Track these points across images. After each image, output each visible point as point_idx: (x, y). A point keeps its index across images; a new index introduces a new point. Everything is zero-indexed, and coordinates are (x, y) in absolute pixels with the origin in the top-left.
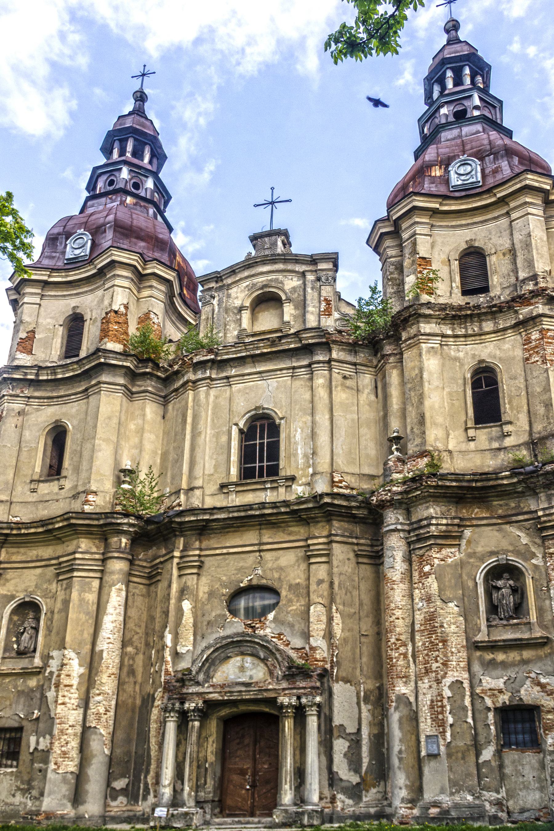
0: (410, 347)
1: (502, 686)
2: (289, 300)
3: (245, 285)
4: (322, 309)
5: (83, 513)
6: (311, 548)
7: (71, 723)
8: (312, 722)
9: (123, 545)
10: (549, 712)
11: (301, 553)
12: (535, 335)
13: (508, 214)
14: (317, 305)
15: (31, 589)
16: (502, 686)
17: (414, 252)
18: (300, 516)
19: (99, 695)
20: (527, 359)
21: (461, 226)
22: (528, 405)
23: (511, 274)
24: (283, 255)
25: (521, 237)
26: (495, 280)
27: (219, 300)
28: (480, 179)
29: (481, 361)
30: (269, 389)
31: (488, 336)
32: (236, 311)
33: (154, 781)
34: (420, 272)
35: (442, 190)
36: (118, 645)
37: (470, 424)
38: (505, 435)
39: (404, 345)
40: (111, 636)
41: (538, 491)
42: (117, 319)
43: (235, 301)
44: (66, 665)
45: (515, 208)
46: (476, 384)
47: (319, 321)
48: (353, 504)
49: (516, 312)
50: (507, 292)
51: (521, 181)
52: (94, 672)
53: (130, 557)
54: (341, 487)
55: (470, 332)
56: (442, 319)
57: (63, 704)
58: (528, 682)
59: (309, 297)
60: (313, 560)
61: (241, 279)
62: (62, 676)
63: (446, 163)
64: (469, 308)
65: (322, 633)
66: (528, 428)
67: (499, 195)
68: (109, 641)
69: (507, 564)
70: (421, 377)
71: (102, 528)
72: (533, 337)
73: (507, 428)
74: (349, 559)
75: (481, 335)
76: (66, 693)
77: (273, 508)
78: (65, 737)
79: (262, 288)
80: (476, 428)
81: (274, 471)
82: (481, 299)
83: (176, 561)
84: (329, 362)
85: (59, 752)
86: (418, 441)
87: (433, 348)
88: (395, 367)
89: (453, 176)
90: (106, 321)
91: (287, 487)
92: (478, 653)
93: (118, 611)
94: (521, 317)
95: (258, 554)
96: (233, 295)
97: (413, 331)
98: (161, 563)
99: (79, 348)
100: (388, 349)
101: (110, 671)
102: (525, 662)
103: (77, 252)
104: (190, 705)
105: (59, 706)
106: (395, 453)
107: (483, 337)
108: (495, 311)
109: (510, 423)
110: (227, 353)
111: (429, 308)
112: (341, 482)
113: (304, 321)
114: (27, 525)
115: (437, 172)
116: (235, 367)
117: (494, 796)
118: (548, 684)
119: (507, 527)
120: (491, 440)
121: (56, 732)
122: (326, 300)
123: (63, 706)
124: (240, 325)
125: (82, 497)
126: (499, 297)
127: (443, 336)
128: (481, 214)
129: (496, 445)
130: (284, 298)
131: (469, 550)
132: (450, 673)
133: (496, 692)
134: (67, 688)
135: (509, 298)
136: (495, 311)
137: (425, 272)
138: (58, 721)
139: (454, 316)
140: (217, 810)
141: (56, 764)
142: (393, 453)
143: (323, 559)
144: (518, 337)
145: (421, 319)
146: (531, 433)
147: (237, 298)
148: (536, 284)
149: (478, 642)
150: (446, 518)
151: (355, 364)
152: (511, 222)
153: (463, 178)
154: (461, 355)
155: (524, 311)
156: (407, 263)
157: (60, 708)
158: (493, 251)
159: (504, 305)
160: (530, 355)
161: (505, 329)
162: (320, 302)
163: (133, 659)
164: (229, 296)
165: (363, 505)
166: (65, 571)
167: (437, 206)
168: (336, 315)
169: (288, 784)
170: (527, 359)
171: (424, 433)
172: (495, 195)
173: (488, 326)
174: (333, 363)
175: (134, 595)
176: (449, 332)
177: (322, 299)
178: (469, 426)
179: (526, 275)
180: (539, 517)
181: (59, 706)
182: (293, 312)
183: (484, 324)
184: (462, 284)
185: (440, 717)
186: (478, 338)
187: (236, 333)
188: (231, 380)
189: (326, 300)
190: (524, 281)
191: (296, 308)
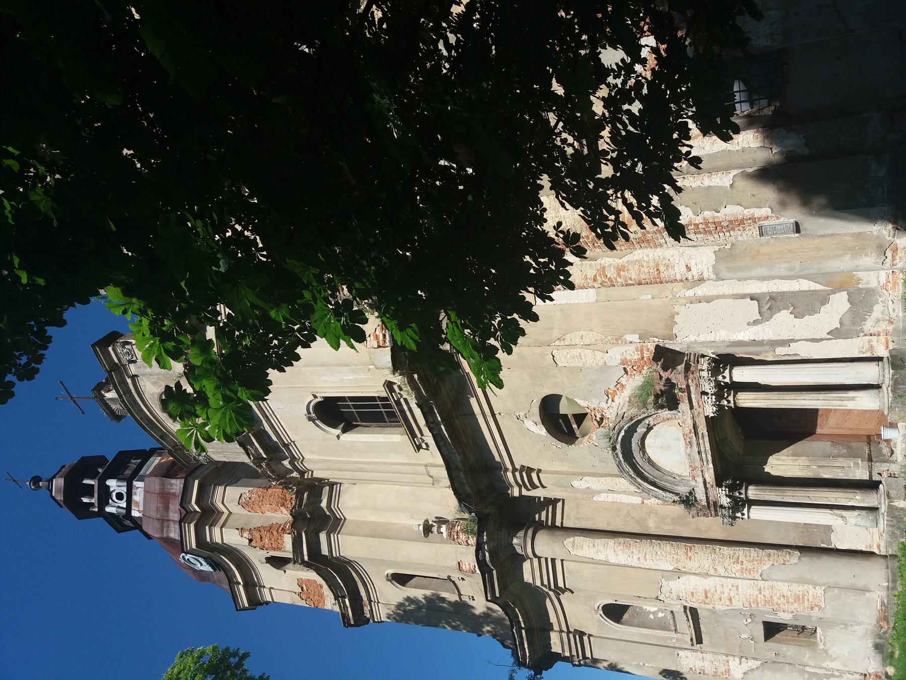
57: (730, 600)
68: (642, 559)
76: (716, 597)
78: (775, 598)
83: (525, 492)
85: (796, 605)
93: (601, 548)
101: (683, 558)
141: (812, 609)
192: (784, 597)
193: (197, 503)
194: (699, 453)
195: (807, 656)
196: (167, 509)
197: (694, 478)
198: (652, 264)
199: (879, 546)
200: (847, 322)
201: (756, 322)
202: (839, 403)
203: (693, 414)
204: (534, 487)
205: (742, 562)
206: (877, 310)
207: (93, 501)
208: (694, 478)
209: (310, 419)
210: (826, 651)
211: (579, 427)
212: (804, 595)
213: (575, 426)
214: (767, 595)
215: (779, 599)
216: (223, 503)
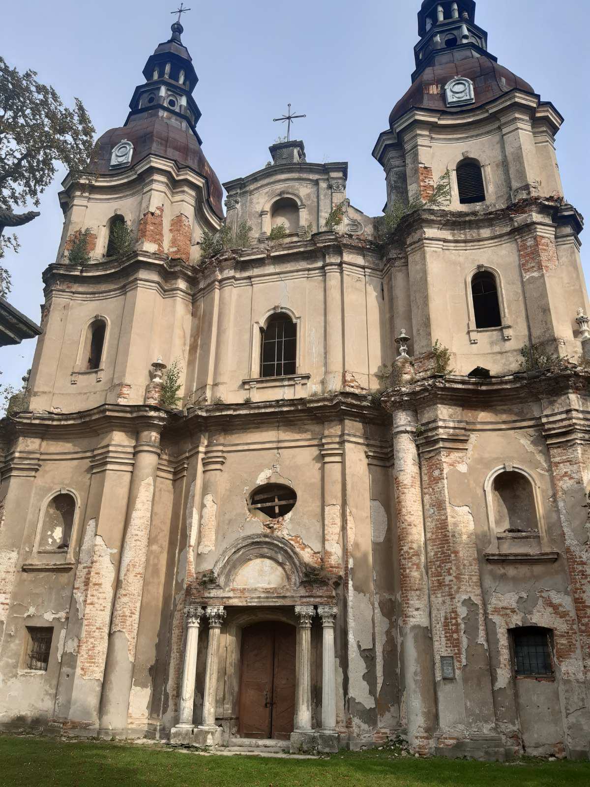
0: (414, 251)
1: (514, 605)
3: (265, 191)
5: (118, 405)
6: (326, 447)
7: (98, 625)
8: (329, 636)
9: (153, 438)
10: (562, 636)
11: (315, 451)
12: (530, 242)
13: (499, 128)
15: (67, 482)
16: (514, 605)
18: (315, 415)
19: (125, 595)
20: (524, 265)
22: (526, 310)
24: (299, 164)
25: (512, 150)
27: (242, 205)
28: (473, 96)
30: (288, 290)
31: (486, 242)
33: (175, 693)
34: (423, 181)
35: (439, 105)
36: (145, 542)
37: (473, 326)
38: (506, 339)
39: (409, 249)
41: (540, 396)
43: (257, 206)
44: (96, 562)
49: (511, 219)
53: (159, 451)
54: (352, 387)
55: (469, 238)
56: (444, 225)
57: (92, 604)
58: (540, 602)
59: (321, 203)
60: (327, 459)
62: (92, 574)
63: (442, 82)
65: (336, 537)
66: (526, 333)
67: (491, 111)
68: (137, 538)
69: (514, 472)
70: (426, 280)
71: (135, 422)
72: (528, 244)
73: (507, 332)
74: (360, 460)
75: (479, 241)
76: (95, 593)
77: (290, 405)
78: (92, 640)
79: (280, 195)
80: (478, 332)
81: (291, 368)
82: (478, 206)
84: (340, 265)
86: (424, 343)
87: (436, 252)
88: (400, 271)
89: (449, 94)
91: (303, 385)
92: (490, 567)
93: (146, 507)
94: (516, 224)
95: (276, 451)
96: (255, 201)
97: (416, 236)
98: (187, 458)
100: (393, 254)
102: (537, 578)
103: (120, 159)
104: (211, 611)
105: (87, 606)
106: (403, 354)
107: (481, 243)
108: (490, 219)
109: (509, 327)
110: (249, 255)
111: (432, 214)
112: (352, 381)
114: (67, 417)
115: (434, 90)
116: (257, 267)
117: (511, 728)
118: (560, 605)
119: (512, 432)
120: (492, 343)
121: (83, 634)
123: (91, 606)
125: (117, 390)
126: (495, 206)
127: (445, 241)
129: (497, 349)
130: (299, 203)
131: (476, 456)
132: (464, 588)
133: (508, 611)
134: (97, 587)
136: (490, 219)
137: (427, 180)
138: (85, 622)
139: (454, 222)
140: (234, 730)
141: (82, 669)
142: (401, 354)
143: (338, 459)
144: (514, 245)
145: (423, 225)
147: (258, 203)
148: (529, 193)
149: (489, 555)
150: (454, 421)
153: (457, 95)
154: (461, 259)
155: (520, 219)
157: (89, 609)
160: (527, 261)
161: (501, 236)
163: (158, 559)
166: (98, 464)
167: (435, 120)
169: (306, 704)
171: (429, 334)
173: (485, 232)
174: (344, 265)
175: (160, 490)
176: (450, 238)
178: (471, 329)
179: (519, 185)
180: (543, 424)
181: (87, 606)
182: (308, 217)
183: (482, 231)
185: (455, 636)
186: (476, 243)
188: (252, 280)
190: (517, 190)
191: (310, 213)
192: (93, 647)
194: (259, 597)
195: (10, 661)
196: (176, 148)
197: (233, 590)
198: (421, 586)
199: (132, 723)
200: (359, 707)
201: (359, 646)
202: (305, 700)
203: (297, 597)
204: (204, 465)
205: (130, 617)
206: (365, 726)
207: (166, 76)
208: (233, 590)
209: (274, 309)
210: (15, 676)
211: (258, 509)
212: (94, 663)
213: (259, 505)
214: (97, 634)
215: (92, 643)
216: (183, 201)
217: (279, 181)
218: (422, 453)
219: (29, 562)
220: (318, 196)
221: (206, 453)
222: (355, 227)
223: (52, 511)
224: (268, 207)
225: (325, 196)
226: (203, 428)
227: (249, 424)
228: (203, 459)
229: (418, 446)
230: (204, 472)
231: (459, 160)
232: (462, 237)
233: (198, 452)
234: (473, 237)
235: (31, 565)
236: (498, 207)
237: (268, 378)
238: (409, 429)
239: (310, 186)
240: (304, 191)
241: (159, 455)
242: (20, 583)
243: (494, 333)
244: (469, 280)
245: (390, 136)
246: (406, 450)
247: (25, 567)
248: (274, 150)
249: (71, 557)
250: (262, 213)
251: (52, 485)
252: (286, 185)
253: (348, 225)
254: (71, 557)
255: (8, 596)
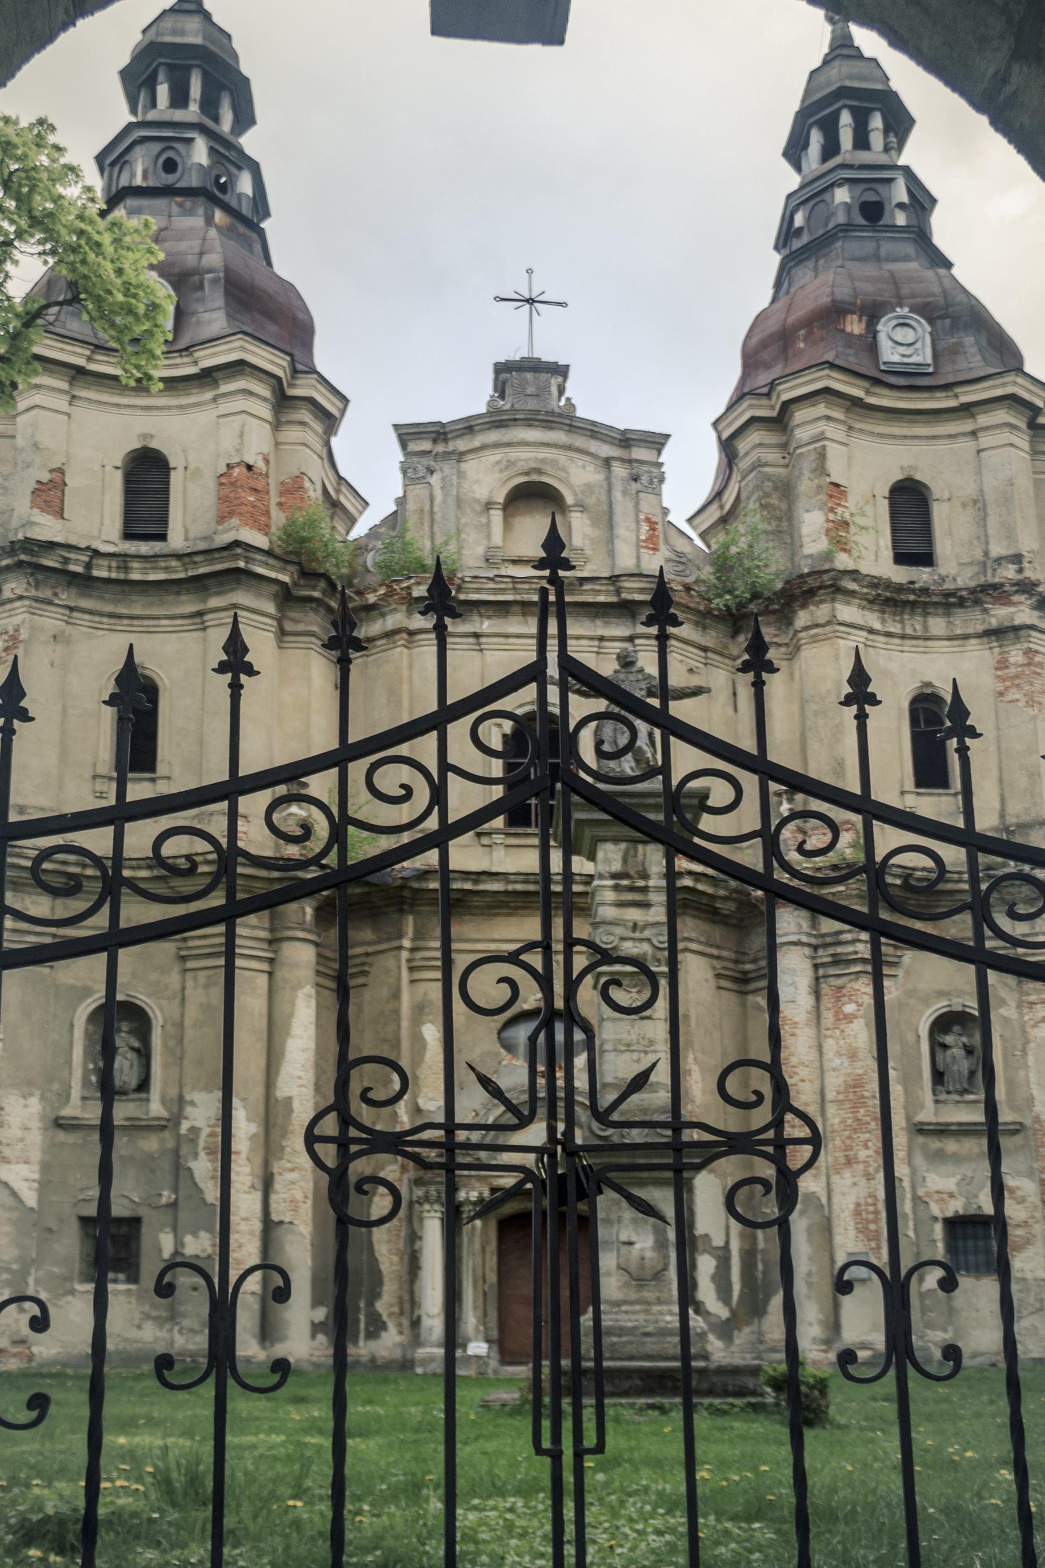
2: (582, 507)
4: (643, 537)
14: (633, 526)
17: (821, 468)
20: (1001, 694)
21: (894, 437)
23: (975, 542)
26: (944, 546)
29: (929, 684)
32: (478, 508)
40: (301, 1074)
42: (253, 483)
45: (987, 428)
46: (914, 721)
47: (638, 557)
48: (722, 892)
49: (986, 611)
50: (969, 572)
51: (1004, 385)
52: (275, 1134)
59: (618, 509)
61: (484, 447)
64: (913, 591)
68: (300, 1082)
75: (927, 639)
80: (918, 794)
82: (923, 576)
90: (225, 479)
99: (164, 520)
107: (930, 643)
113: (612, 554)
122: (648, 520)
124: (489, 537)
126: (955, 580)
128: (927, 423)
130: (569, 500)
135: (972, 584)
144: (987, 653)
146: (1002, 816)
151: (705, 649)
152: (979, 452)
156: (805, 485)
158: (946, 496)
159: (964, 593)
160: (1006, 688)
161: (966, 637)
162: (638, 522)
164: (461, 475)
165: (734, 895)
168: (664, 552)
170: (1001, 694)
172: (956, 396)
173: (937, 625)
177: (642, 517)
178: (907, 788)
182: (589, 530)
184: (895, 541)
186: (921, 643)
187: (481, 550)
189: (648, 520)
191: (595, 524)
193: (310, 400)
204: (411, 969)
217: (527, 444)
218: (825, 977)
219: (66, 1112)
220: (610, 490)
221: (412, 950)
222: (681, 568)
223: (91, 1028)
224: (500, 498)
225: (625, 493)
226: (406, 907)
227: (499, 907)
228: (409, 961)
229: (816, 967)
230: (413, 982)
231: (894, 480)
232: (895, 628)
233: (400, 948)
234: (915, 630)
235: (76, 1118)
236: (960, 583)
237: (521, 830)
238: (804, 939)
239: (591, 468)
240: (577, 476)
241: (317, 945)
242: (51, 1148)
243: (943, 798)
244: (906, 705)
245: (764, 402)
246: (794, 972)
247: (62, 1122)
248: (506, 373)
249: (156, 1108)
250: (488, 506)
251: (90, 984)
252: (541, 456)
253: (668, 560)
254: (156, 1108)
255: (36, 1168)
